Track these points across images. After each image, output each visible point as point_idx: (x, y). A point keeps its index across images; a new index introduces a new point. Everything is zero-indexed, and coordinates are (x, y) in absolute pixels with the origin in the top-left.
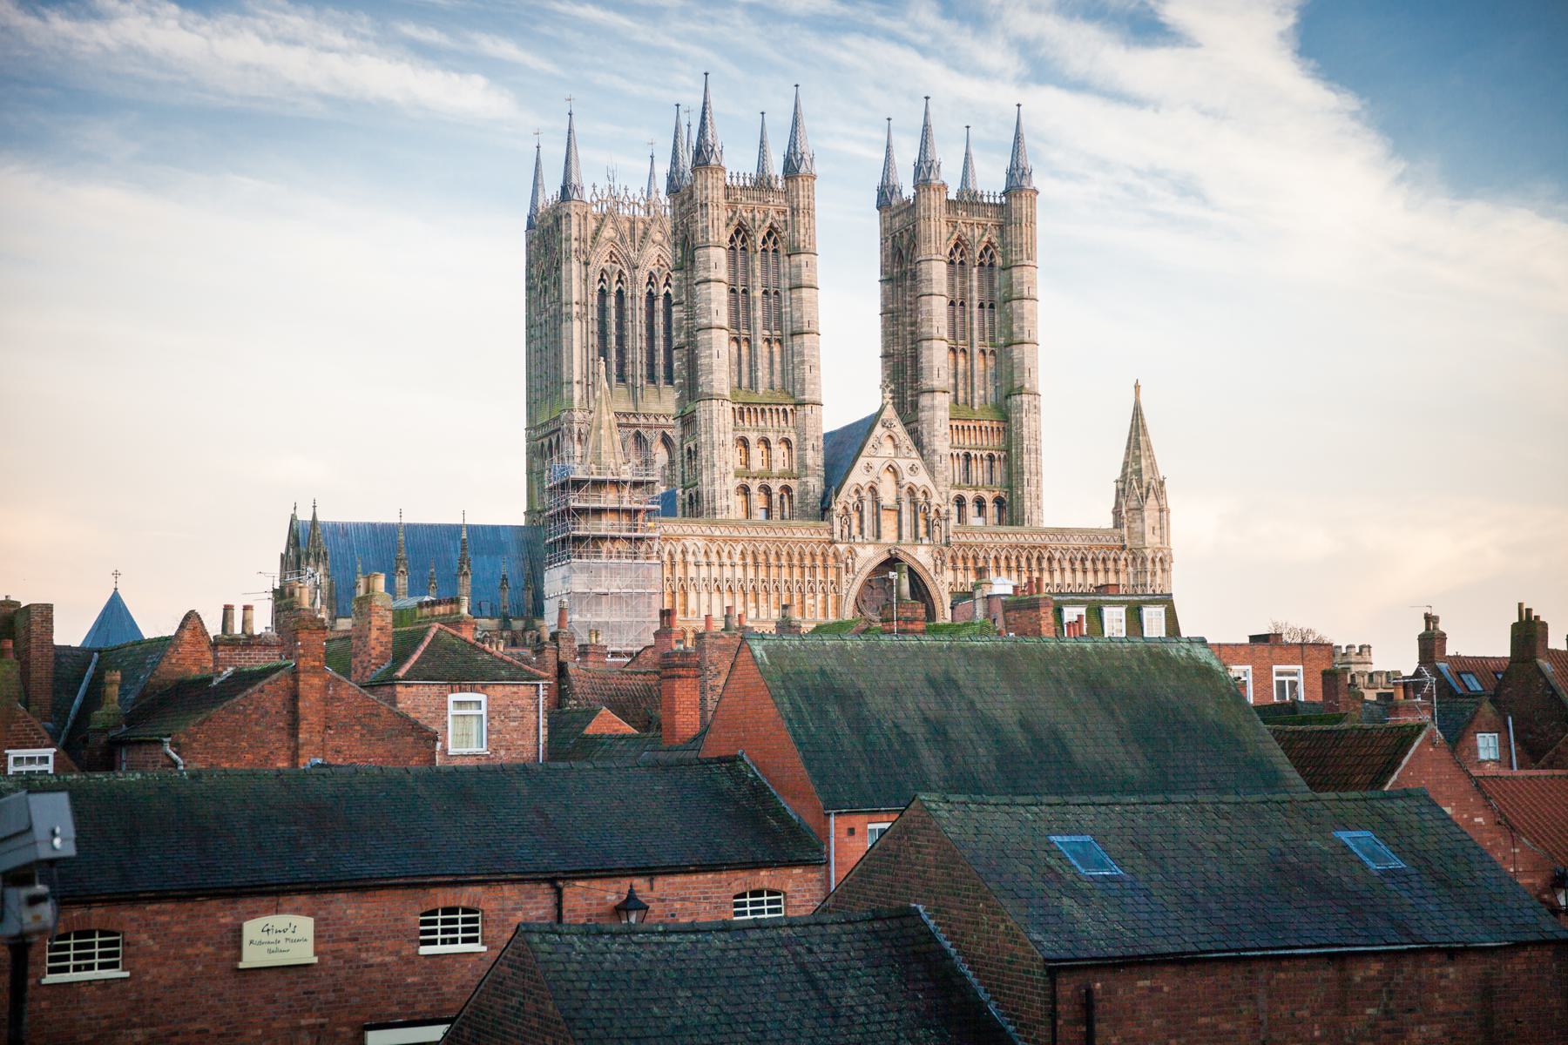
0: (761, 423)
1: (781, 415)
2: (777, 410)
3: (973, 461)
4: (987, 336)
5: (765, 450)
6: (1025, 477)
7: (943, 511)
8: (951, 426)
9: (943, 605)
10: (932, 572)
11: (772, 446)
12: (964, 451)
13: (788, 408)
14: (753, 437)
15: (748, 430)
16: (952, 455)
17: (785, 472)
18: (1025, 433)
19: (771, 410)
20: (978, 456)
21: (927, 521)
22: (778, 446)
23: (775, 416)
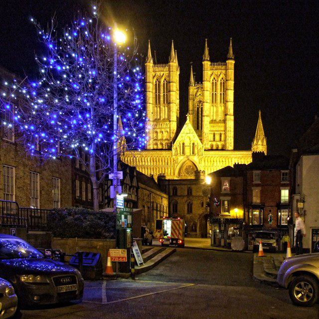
14: (159, 131)
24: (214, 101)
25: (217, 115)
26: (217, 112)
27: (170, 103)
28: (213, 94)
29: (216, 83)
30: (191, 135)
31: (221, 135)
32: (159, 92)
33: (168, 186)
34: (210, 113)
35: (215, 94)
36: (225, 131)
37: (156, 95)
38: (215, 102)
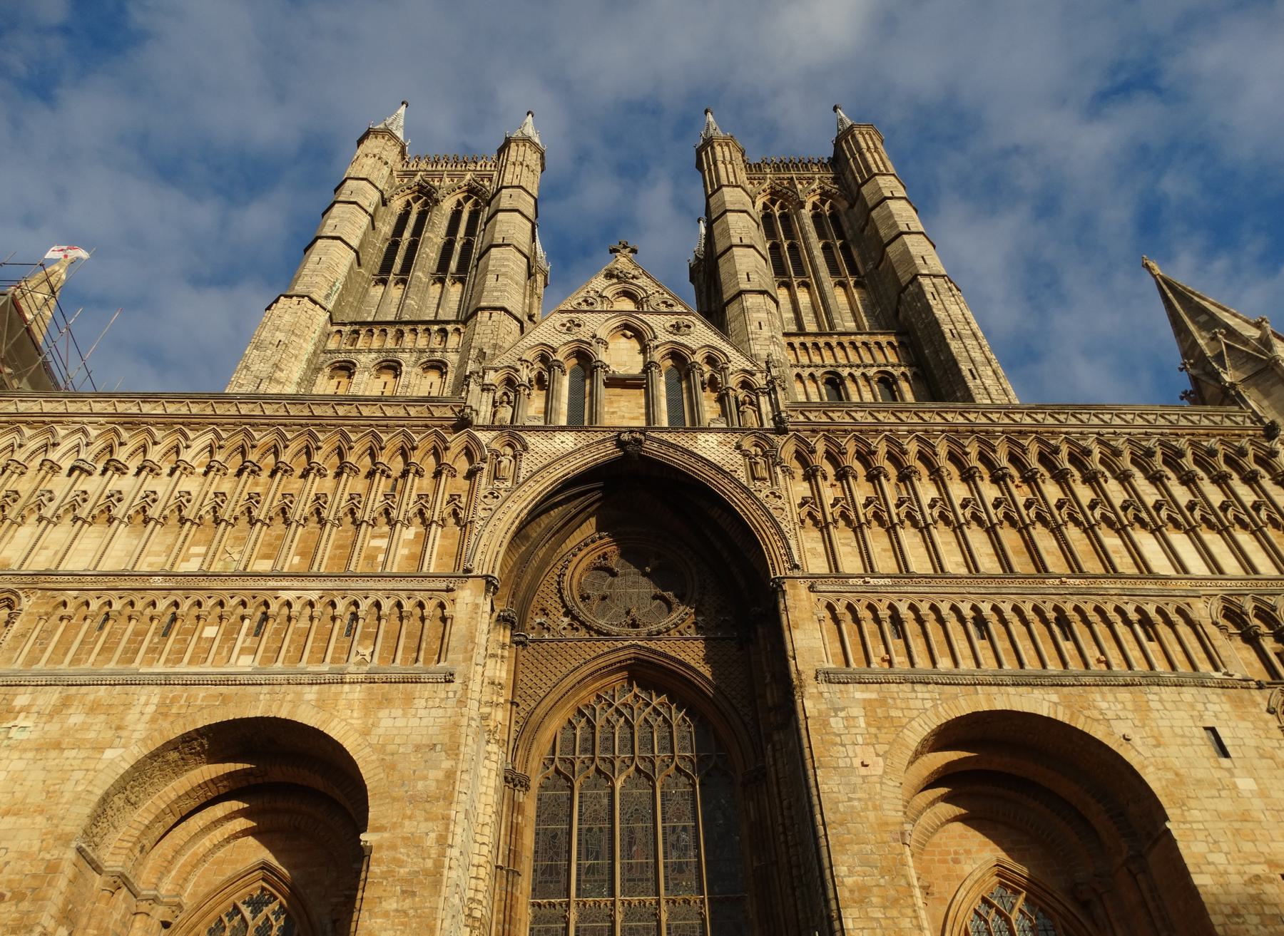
0: (390, 343)
2: (427, 330)
3: (849, 385)
6: (963, 367)
7: (760, 380)
8: (791, 345)
9: (784, 538)
10: (742, 475)
11: (404, 368)
12: (822, 370)
13: (450, 328)
15: (359, 351)
18: (940, 314)
19: (414, 330)
21: (721, 400)
22: (420, 370)
38: (800, 271)
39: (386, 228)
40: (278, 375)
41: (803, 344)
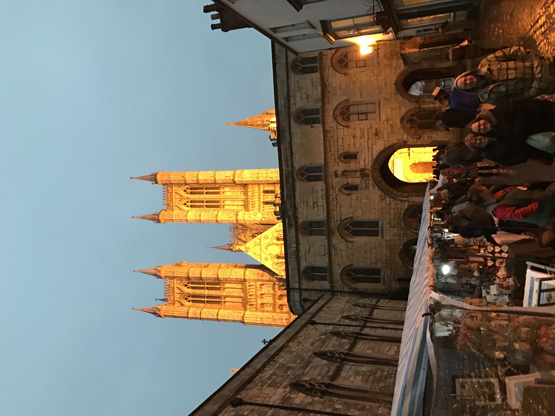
1: (251, 287)
4: (216, 191)
5: (265, 295)
8: (252, 210)
11: (263, 293)
12: (262, 205)
13: (248, 285)
14: (260, 301)
15: (257, 303)
16: (263, 210)
17: (273, 287)
18: (250, 179)
19: (249, 292)
20: (263, 198)
22: (263, 290)
23: (252, 290)
24: (214, 205)
25: (236, 199)
26: (231, 199)
27: (218, 279)
28: (207, 206)
29: (191, 202)
30: (264, 242)
31: (266, 192)
32: (203, 297)
33: (305, 295)
34: (233, 210)
35: (206, 202)
36: (259, 184)
37: (207, 302)
38: (218, 202)
39: (202, 305)
40: (271, 317)
41: (252, 207)
